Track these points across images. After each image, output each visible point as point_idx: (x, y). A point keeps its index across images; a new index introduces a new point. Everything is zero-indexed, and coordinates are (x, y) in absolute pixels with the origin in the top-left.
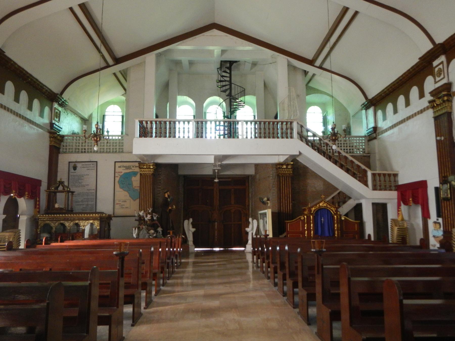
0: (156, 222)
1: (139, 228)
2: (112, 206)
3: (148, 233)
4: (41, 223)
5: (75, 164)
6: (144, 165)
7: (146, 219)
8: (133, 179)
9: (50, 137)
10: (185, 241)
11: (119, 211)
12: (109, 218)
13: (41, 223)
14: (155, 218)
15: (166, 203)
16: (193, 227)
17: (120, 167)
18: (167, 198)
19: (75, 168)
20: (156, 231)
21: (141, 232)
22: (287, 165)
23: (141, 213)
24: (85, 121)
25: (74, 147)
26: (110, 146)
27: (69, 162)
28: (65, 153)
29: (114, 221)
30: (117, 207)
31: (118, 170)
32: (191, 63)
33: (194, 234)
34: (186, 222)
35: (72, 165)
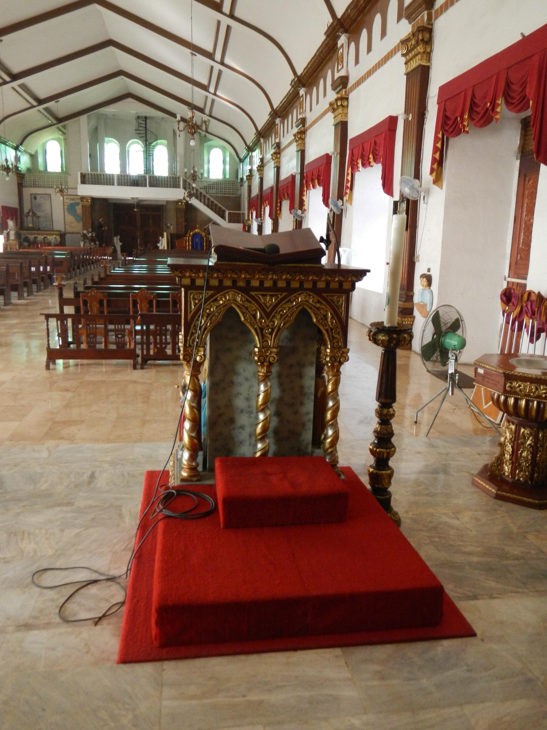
0: (95, 238)
1: (84, 241)
2: (64, 226)
3: (90, 244)
4: (23, 237)
5: (35, 196)
6: (84, 199)
7: (88, 235)
8: (77, 207)
9: (17, 177)
10: (115, 251)
11: (69, 229)
12: (65, 234)
13: (23, 237)
14: (94, 235)
15: (101, 226)
16: (120, 242)
17: (67, 199)
18: (101, 222)
19: (35, 198)
20: (95, 244)
21: (86, 244)
22: (182, 203)
23: (85, 232)
24: (33, 157)
25: (33, 183)
26: (53, 178)
27: (31, 194)
28: (26, 187)
29: (68, 237)
30: (67, 227)
31: (65, 201)
32: (114, 115)
33: (121, 247)
34: (115, 238)
35: (33, 196)
